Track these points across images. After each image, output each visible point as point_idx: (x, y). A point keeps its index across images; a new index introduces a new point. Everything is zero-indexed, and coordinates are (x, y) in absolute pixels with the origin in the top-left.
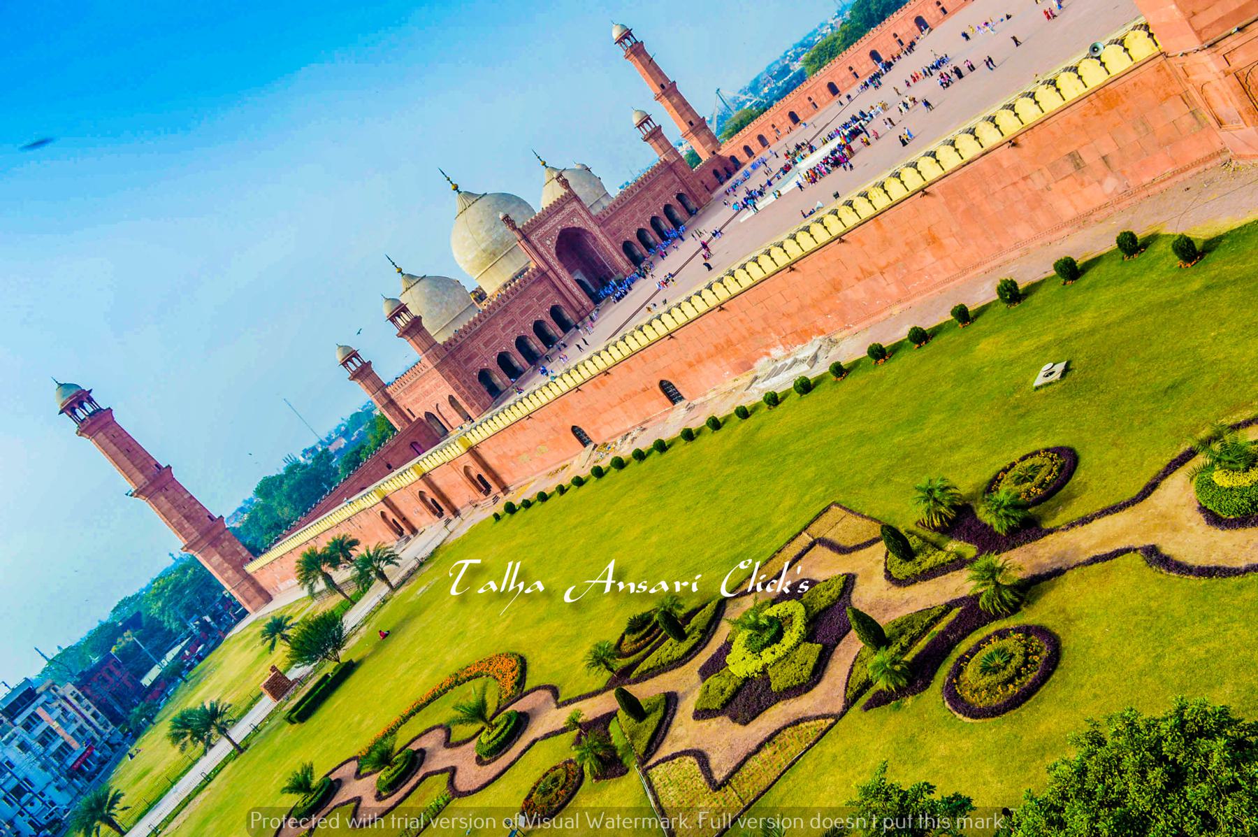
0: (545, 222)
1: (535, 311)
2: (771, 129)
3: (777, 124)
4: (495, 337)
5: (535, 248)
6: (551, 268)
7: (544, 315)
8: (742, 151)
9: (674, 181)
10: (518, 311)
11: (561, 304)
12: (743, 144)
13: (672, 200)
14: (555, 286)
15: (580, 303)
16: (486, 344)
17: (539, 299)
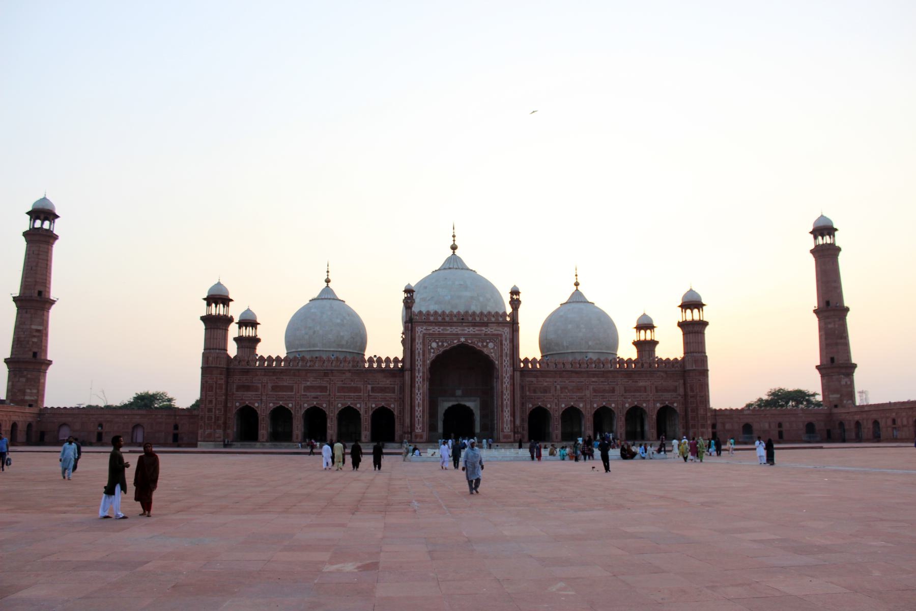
0: (451, 324)
1: (359, 398)
2: (889, 422)
3: (899, 422)
4: (290, 389)
5: (413, 340)
6: (412, 369)
7: (365, 409)
8: (853, 425)
9: (675, 390)
10: (339, 384)
11: (396, 413)
12: (857, 418)
13: (652, 408)
14: (402, 389)
15: (412, 426)
16: (274, 388)
17: (373, 390)
